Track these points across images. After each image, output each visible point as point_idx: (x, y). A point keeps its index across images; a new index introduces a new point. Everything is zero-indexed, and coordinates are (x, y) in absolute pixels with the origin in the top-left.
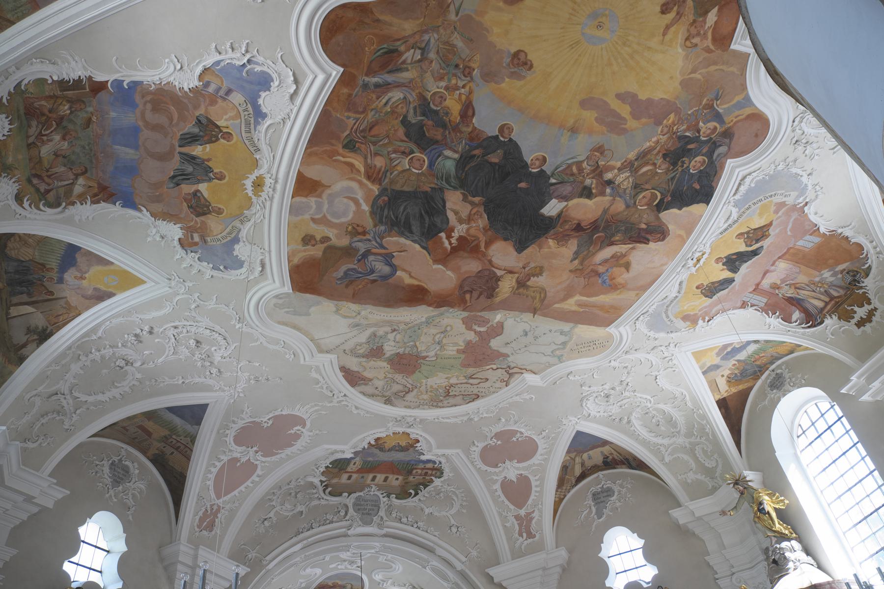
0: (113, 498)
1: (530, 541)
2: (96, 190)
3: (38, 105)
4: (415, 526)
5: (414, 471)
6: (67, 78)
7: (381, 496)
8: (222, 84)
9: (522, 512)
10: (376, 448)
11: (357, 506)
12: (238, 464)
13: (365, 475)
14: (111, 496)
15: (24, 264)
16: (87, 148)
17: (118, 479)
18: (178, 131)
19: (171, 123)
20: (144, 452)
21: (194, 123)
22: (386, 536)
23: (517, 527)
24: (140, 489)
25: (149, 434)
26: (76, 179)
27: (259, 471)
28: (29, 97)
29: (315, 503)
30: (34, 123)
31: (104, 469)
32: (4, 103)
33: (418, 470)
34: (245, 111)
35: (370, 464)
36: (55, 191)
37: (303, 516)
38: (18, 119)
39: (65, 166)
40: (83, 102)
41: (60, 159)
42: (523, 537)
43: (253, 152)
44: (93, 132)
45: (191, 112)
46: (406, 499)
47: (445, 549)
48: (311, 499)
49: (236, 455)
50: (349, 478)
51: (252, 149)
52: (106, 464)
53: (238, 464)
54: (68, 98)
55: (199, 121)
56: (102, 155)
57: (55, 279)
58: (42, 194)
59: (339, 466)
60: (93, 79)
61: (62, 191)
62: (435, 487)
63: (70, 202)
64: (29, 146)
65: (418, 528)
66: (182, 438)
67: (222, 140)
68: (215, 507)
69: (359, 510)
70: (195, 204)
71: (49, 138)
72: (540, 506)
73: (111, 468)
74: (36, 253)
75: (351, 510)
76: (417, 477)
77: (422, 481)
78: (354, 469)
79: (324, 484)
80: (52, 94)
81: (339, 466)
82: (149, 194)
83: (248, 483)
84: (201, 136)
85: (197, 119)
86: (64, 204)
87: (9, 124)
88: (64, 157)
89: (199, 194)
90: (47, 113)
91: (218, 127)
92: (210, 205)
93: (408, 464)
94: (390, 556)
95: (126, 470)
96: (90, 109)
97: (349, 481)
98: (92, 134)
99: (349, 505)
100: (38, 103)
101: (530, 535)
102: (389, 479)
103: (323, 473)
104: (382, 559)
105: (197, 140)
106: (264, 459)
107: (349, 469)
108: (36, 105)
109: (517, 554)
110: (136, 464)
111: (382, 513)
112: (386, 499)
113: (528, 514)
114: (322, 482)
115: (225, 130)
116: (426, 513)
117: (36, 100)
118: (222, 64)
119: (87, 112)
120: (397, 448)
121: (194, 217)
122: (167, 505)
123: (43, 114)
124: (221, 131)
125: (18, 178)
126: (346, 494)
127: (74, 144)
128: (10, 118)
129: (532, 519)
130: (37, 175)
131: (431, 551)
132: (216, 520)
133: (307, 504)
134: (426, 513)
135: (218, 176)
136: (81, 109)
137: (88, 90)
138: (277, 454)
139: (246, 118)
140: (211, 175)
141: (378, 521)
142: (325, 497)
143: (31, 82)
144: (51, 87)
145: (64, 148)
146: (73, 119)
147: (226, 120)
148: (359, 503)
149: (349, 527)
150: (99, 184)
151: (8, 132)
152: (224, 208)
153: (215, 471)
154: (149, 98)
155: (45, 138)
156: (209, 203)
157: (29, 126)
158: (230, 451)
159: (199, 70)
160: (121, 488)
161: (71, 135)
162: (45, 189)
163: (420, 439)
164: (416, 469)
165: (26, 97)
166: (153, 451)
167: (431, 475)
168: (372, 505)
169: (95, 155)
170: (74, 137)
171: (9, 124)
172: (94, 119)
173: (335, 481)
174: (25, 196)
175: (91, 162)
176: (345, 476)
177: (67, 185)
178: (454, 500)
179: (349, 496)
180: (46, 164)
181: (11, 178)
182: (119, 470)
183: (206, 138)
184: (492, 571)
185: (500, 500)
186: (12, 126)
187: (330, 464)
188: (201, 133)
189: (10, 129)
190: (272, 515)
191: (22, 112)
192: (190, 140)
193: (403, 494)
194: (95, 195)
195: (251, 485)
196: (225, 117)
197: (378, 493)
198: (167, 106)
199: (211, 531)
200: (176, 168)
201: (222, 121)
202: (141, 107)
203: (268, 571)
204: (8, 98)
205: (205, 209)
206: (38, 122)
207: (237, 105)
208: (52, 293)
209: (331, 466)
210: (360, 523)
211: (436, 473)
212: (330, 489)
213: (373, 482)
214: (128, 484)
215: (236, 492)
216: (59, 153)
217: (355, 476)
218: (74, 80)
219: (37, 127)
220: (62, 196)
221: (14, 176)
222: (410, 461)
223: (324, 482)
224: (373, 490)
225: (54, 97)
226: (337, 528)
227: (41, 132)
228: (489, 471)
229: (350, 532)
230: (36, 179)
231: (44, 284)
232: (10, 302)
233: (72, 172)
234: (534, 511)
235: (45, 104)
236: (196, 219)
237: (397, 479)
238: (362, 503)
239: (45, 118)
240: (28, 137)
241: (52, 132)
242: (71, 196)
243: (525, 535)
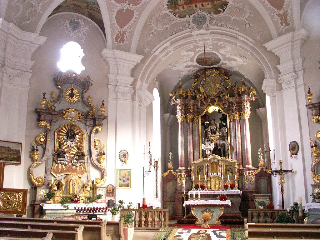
0: (74, 36)
1: (287, 27)
4: (225, 26)
7: (206, 14)
9: (281, 12)
11: (194, 21)
12: (124, 12)
14: (73, 35)
17: (75, 28)
20: (83, 14)
22: (212, 33)
23: (280, 21)
24: (87, 30)
25: (79, 7)
27: (136, 13)
29: (173, 22)
31: (67, 25)
37: (168, 30)
42: (283, 26)
47: (242, 37)
48: (170, 21)
49: (120, 8)
50: (183, 8)
52: (67, 22)
53: (124, 12)
59: (173, 3)
62: (232, 5)
65: (227, 27)
66: (93, 5)
68: (122, 32)
72: (291, 7)
73: (70, 24)
75: (192, 23)
77: (222, 3)
79: (173, 13)
81: (173, 3)
83: (133, 19)
94: (222, 43)
95: (78, 24)
99: (190, 21)
101: (287, 24)
104: (219, 44)
106: (135, 7)
107: (180, 4)
109: (280, 35)
110: (82, 20)
111: (207, 22)
112: (209, 15)
113: (285, 12)
114: (171, 12)
116: (232, 19)
122: (101, 34)
126: (188, 16)
129: (287, 15)
131: (237, 38)
132: (124, 37)
133: (170, 23)
134: (232, 19)
138: (139, 3)
141: (206, 27)
142: (177, 19)
149: (191, 32)
153: (114, 16)
158: (116, 6)
160: (77, 31)
166: (86, 14)
173: (177, 11)
176: (181, 8)
178: (245, 10)
179: (189, 17)
182: (75, 24)
184: (267, 45)
185: (268, 6)
187: (168, 2)
190: (153, 31)
193: (217, 12)
195: (135, 20)
197: (204, 13)
199: (123, 42)
203: (156, 57)
209: (169, 4)
210: (196, 28)
212: (177, 15)
214: (80, 29)
215: (129, 24)
217: (185, 6)
223: (172, 12)
224: (199, 11)
226: (185, 32)
229: (193, 33)
234: (288, 10)
237: (208, 4)
238: (197, 19)
243: (284, 24)
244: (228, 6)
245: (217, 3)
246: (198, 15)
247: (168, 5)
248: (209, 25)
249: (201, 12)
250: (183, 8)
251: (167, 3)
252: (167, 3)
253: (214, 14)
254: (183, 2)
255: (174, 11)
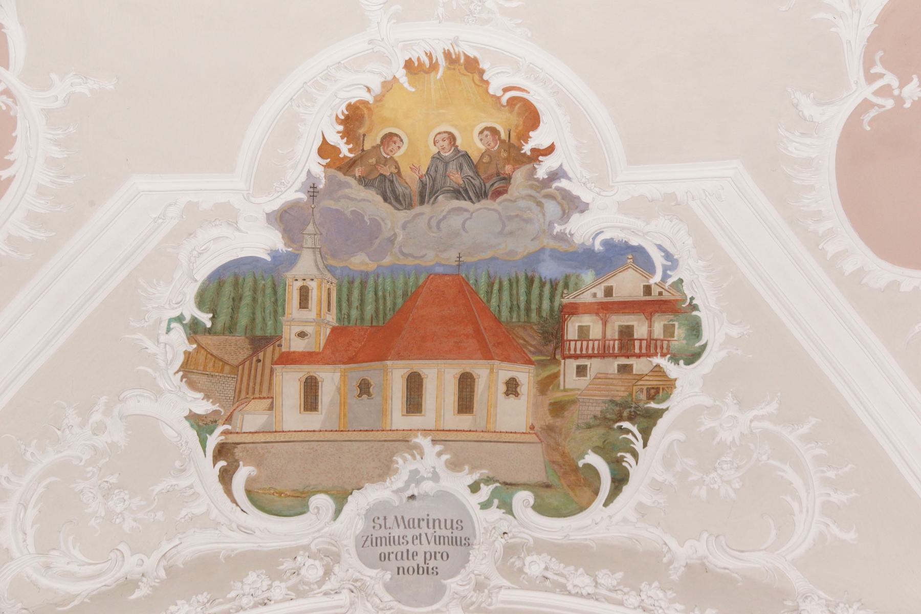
5: (572, 329)
10: (364, 181)
13: (370, 371)
33: (586, 320)
35: (370, 296)
46: (582, 509)
50: (311, 390)
59: (243, 320)
69: (384, 557)
76: (595, 366)
77: (620, 393)
78: (309, 329)
93: (530, 281)
97: (314, 421)
102: (480, 387)
103: (189, 368)
112: (495, 514)
120: (456, 178)
148: (383, 533)
163: (538, 97)
164: (573, 310)
167: (652, 347)
168: (439, 540)
211: (669, 330)
212: (243, 474)
213: (415, 421)
222: (534, 258)
228: (906, 287)
237: (512, 387)
238: (396, 532)
244: (657, 431)
245: (582, 383)
246: (412, 497)
247: (194, 329)
248: (497, 580)
249: (435, 477)
250: (311, 390)
251: (191, 310)
252: (191, 310)
253: (541, 508)
254: (319, 322)
255: (229, 420)
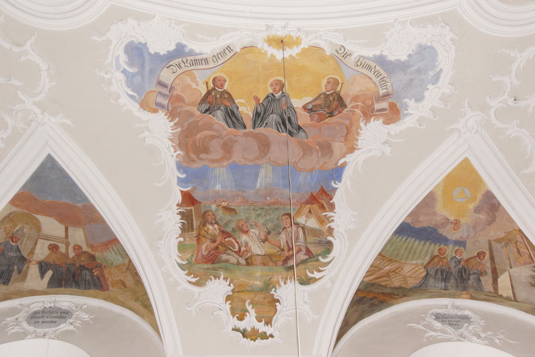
2: (315, 207)
3: (205, 251)
6: (180, 225)
8: (154, 91)
15: (432, 272)
16: (259, 212)
18: (225, 130)
19: (218, 137)
21: (210, 116)
26: (297, 224)
28: (196, 259)
30: (224, 257)
32: (197, 281)
34: (180, 67)
36: (308, 245)
38: (217, 270)
39: (280, 233)
40: (205, 212)
41: (269, 237)
43: (233, 53)
44: (240, 206)
45: (199, 119)
51: (229, 55)
54: (200, 225)
55: (206, 111)
56: (268, 198)
57: (457, 248)
58: (310, 258)
60: (180, 203)
61: (310, 239)
63: (328, 232)
64: (248, 263)
67: (226, 87)
70: (327, 110)
71: (244, 245)
74: (415, 262)
80: (195, 239)
82: (320, 154)
84: (226, 108)
85: (204, 113)
86: (329, 238)
87: (219, 279)
88: (269, 233)
89: (310, 106)
90: (215, 244)
91: (209, 93)
92: (324, 94)
96: (214, 207)
98: (242, 207)
100: (204, 251)
105: (233, 112)
108: (205, 253)
115: (211, 85)
117: (200, 252)
118: (131, 93)
119: (217, 210)
121: (346, 109)
123: (217, 248)
124: (214, 89)
125: (282, 278)
127: (254, 223)
128: (213, 278)
130: (284, 260)
135: (278, 88)
136: (213, 214)
137: (192, 208)
139: (189, 65)
140: (277, 95)
143: (180, 255)
144: (188, 239)
145: (257, 232)
146: (224, 222)
147: (197, 85)
150: (307, 203)
151: (226, 281)
152: (326, 78)
154: (194, 156)
155: (243, 249)
156: (321, 95)
157: (227, 261)
159: (145, 115)
161: (242, 225)
162: (305, 254)
165: (195, 261)
169: (268, 205)
170: (245, 222)
171: (219, 279)
172: (225, 204)
174: (306, 275)
175: (277, 209)
177: (304, 233)
180: (274, 250)
181: (280, 285)
183: (228, 104)
186: (222, 277)
188: (222, 108)
189: (224, 279)
191: (210, 266)
192: (234, 119)
194: (322, 207)
196: (194, 86)
198: (197, 140)
200: (276, 131)
201: (199, 88)
202: (205, 163)
204: (192, 276)
205: (331, 98)
206: (224, 253)
207: (175, 75)
208: (481, 255)
216: (263, 237)
218: (181, 219)
219: (229, 255)
220: (318, 239)
221: (278, 282)
225: (199, 238)
227: (236, 252)
230: (289, 261)
231: (465, 258)
232: (491, 293)
233: (288, 227)
235: (205, 245)
236: (349, 107)
239: (220, 246)
240: (238, 264)
241: (237, 242)
242: (320, 231)
